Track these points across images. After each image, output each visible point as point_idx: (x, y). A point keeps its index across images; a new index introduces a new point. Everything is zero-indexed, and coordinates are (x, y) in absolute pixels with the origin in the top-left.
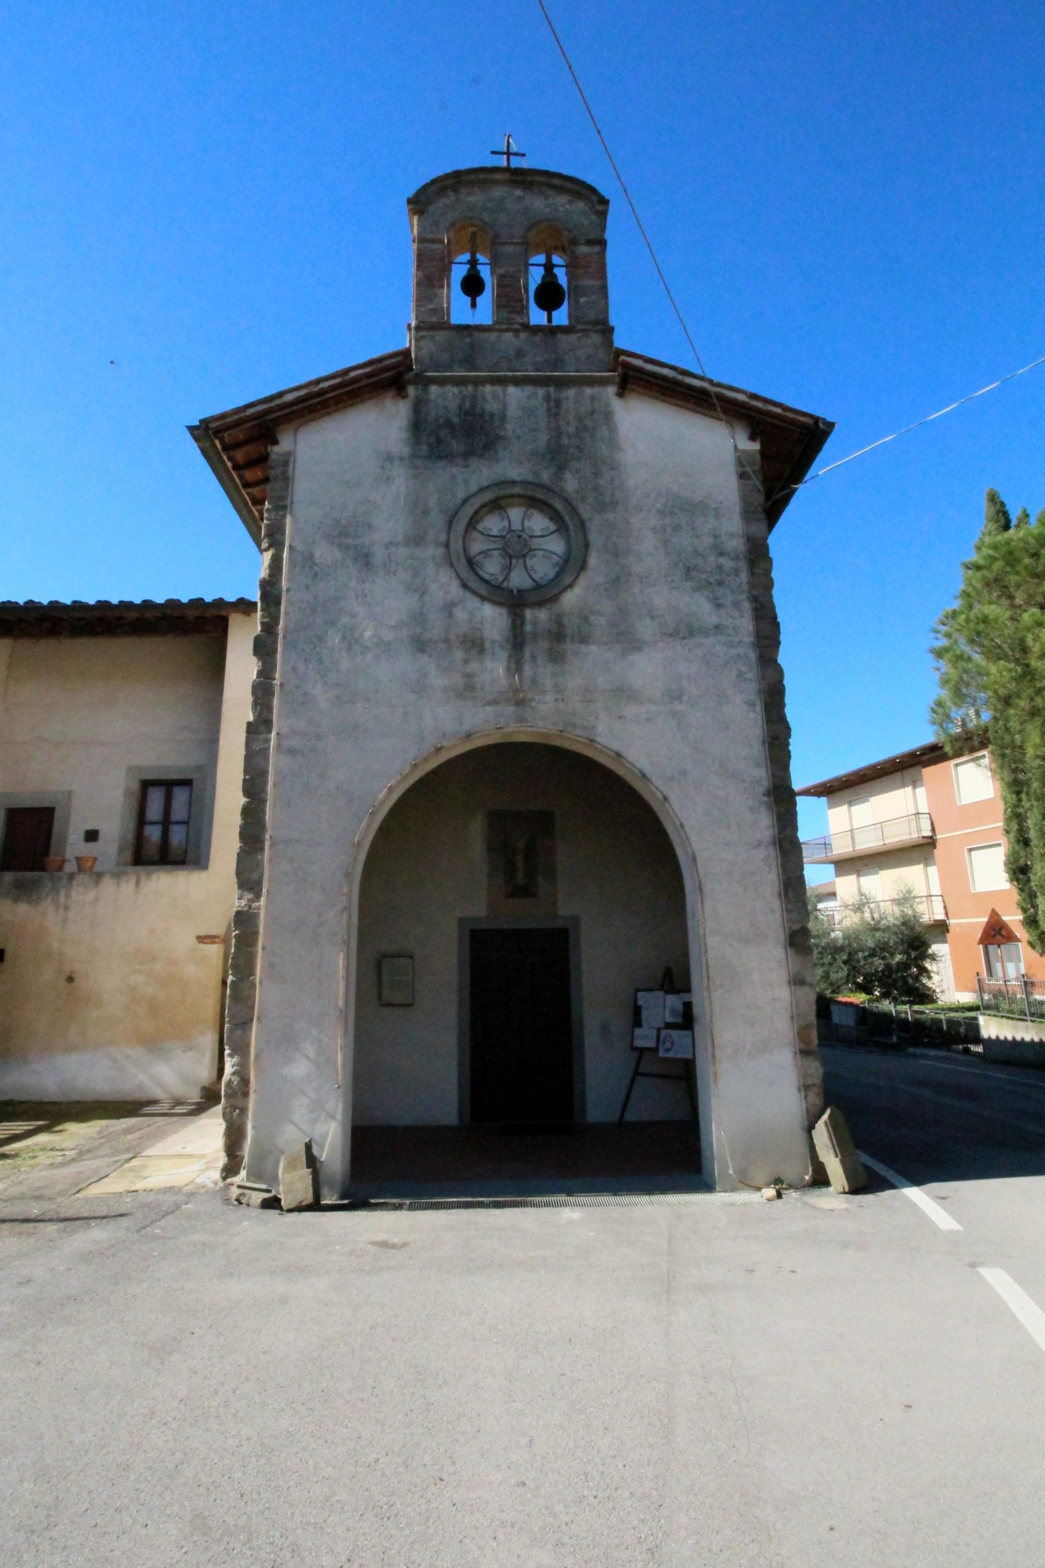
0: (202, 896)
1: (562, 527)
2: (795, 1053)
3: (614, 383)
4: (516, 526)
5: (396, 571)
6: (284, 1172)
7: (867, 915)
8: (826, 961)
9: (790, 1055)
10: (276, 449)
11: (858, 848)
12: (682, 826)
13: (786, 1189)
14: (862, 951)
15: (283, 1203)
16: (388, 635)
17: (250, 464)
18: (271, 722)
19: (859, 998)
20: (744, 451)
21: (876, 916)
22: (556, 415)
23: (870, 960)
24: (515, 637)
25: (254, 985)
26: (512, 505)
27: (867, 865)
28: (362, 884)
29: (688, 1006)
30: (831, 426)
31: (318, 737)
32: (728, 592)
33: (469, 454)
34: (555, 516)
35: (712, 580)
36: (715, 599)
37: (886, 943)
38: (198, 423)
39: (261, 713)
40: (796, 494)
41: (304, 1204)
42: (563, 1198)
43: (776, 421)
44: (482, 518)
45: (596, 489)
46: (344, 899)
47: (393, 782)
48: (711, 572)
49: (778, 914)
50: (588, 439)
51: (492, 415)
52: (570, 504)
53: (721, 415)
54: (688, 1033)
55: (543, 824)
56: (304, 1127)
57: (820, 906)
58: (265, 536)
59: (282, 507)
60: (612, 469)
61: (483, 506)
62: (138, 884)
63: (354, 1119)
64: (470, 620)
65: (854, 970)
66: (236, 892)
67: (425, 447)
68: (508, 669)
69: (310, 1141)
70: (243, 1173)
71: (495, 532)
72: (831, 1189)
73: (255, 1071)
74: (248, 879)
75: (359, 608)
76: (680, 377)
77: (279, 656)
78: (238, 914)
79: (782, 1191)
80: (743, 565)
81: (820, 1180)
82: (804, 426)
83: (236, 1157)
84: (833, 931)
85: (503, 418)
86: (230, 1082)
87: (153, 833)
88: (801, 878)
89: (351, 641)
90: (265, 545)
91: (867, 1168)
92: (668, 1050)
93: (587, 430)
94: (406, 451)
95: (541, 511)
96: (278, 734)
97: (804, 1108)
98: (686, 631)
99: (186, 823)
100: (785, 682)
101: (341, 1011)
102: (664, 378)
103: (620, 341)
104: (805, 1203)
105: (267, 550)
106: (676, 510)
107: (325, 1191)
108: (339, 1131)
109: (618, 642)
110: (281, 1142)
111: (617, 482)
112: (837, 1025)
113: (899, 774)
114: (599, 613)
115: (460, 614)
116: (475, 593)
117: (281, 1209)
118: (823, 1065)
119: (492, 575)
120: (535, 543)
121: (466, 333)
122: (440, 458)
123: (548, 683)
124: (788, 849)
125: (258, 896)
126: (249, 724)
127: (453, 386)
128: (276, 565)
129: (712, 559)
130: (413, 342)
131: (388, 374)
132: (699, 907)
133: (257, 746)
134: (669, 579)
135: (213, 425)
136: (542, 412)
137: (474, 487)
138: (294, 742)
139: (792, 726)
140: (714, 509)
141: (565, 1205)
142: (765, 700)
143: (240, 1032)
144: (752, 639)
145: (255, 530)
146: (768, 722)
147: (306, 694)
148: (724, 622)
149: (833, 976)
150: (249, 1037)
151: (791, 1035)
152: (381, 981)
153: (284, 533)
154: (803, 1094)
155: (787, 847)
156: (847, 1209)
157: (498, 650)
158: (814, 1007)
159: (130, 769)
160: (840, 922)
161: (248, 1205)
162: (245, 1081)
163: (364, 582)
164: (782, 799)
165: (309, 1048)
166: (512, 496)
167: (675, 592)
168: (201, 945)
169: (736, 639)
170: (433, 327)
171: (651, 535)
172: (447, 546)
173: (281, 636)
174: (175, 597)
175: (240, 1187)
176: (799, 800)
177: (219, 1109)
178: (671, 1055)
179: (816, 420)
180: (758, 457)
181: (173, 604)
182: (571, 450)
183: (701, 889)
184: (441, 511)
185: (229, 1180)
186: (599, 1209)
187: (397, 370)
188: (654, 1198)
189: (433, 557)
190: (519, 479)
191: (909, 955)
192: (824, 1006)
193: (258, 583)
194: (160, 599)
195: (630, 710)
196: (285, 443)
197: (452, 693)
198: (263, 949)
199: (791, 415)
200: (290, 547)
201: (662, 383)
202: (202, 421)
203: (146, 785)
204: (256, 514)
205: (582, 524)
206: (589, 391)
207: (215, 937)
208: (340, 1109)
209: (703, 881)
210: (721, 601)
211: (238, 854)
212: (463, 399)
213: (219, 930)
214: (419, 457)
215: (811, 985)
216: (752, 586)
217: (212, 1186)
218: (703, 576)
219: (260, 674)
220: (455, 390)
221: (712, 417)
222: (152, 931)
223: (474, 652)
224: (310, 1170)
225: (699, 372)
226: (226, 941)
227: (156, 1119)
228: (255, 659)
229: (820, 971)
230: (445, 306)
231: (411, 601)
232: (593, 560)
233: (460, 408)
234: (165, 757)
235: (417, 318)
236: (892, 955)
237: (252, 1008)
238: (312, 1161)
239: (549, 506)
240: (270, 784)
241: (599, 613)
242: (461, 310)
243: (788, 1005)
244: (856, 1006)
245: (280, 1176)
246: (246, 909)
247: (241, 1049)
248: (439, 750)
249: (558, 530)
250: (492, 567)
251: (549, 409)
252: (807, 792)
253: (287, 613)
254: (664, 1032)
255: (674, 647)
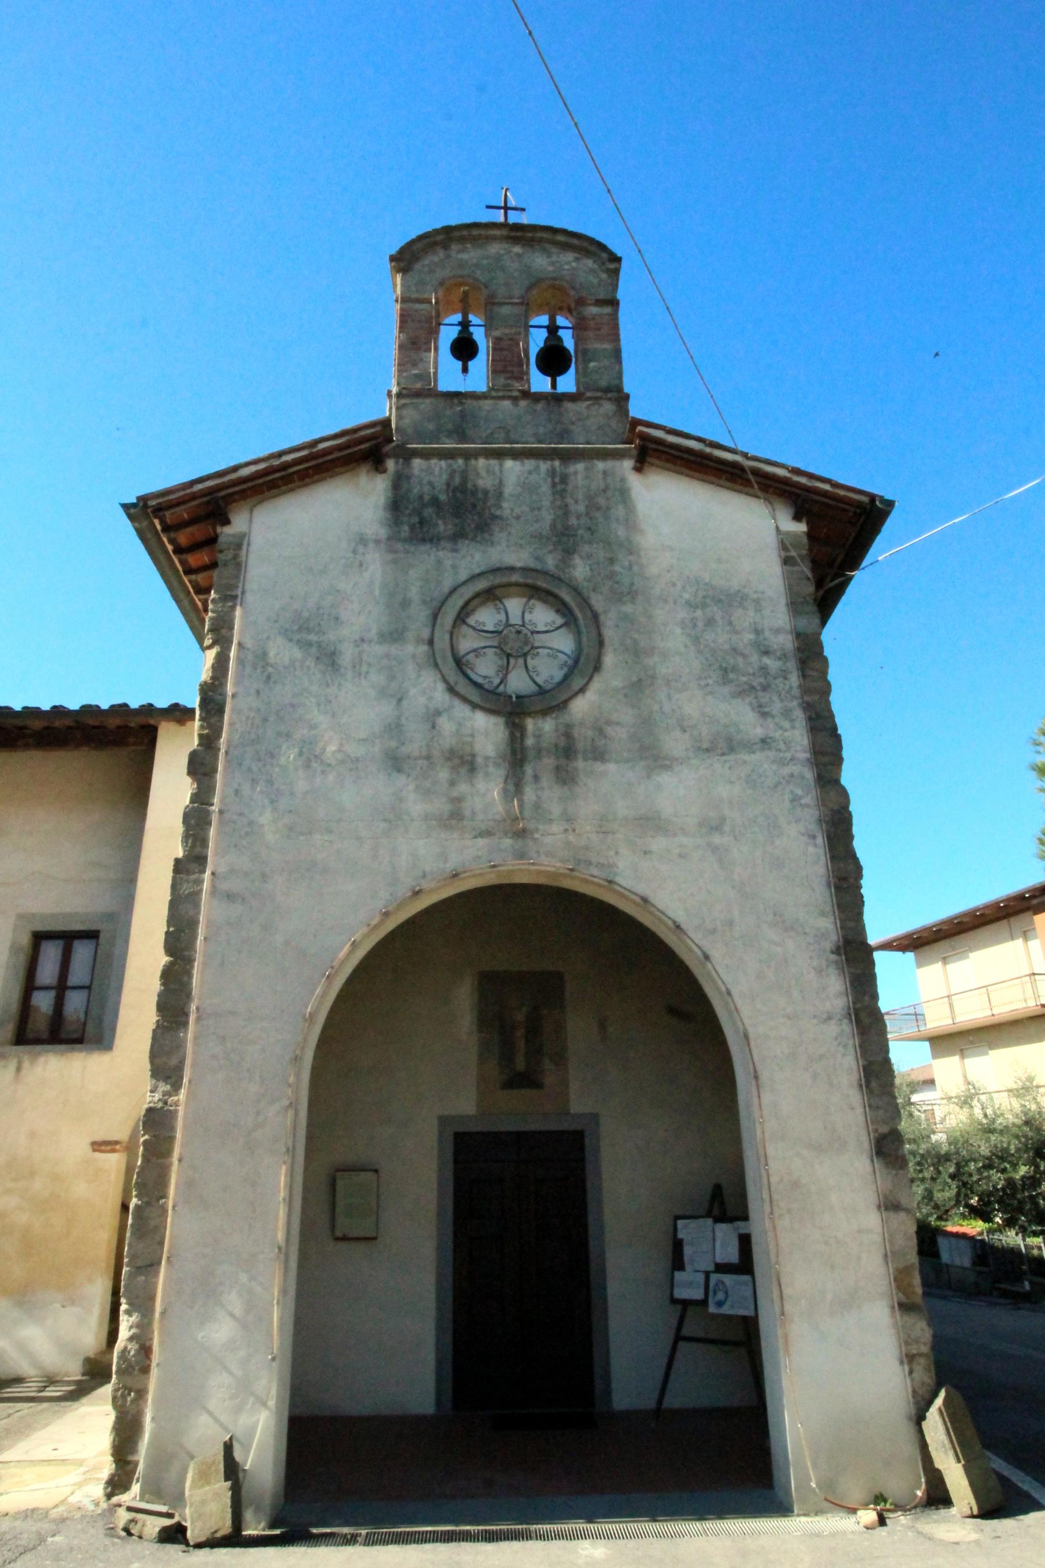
0: (106, 1085)
1: (569, 619)
2: (893, 1307)
3: (630, 457)
4: (515, 619)
5: (368, 672)
6: (193, 1487)
7: (978, 1112)
8: (927, 1174)
9: (886, 1311)
10: (227, 530)
11: (958, 1020)
12: (729, 993)
13: (889, 1510)
14: (975, 1161)
15: (189, 1534)
16: (353, 749)
17: (195, 547)
18: (205, 858)
19: (975, 1227)
20: (788, 533)
21: (989, 1112)
22: (562, 493)
23: (985, 1174)
24: (514, 752)
25: (165, 1211)
26: (508, 596)
27: (972, 1043)
28: (314, 1069)
29: (745, 1242)
30: (890, 504)
31: (264, 877)
32: (775, 698)
33: (458, 536)
34: (562, 608)
35: (755, 684)
36: (760, 706)
37: (1005, 1150)
38: (135, 501)
39: (193, 846)
40: (853, 583)
41: (219, 1535)
42: (581, 1525)
43: (793, 489)
44: (473, 611)
45: (611, 576)
46: (290, 1091)
47: (357, 936)
48: (754, 674)
49: (859, 1110)
50: (601, 520)
51: (486, 492)
52: (580, 594)
53: (760, 493)
54: (747, 1278)
55: (547, 990)
56: (223, 1418)
57: (915, 1098)
58: (209, 631)
59: (231, 597)
60: (631, 554)
61: (477, 595)
62: (19, 1069)
63: (293, 1405)
64: (458, 731)
65: (966, 1187)
66: (148, 1082)
67: (406, 528)
68: (505, 791)
69: (231, 1439)
70: (136, 1488)
71: (490, 627)
72: (954, 1511)
73: (160, 1336)
74: (165, 1065)
75: (317, 716)
76: (708, 450)
77: (219, 776)
78: (150, 1111)
79: (886, 1514)
80: (792, 665)
81: (938, 1497)
82: (859, 505)
83: (129, 1463)
84: (934, 1133)
85: (500, 495)
86: (125, 1350)
87: (43, 1002)
88: (887, 1062)
89: (310, 757)
90: (208, 642)
91: (1003, 1479)
92: (720, 1304)
93: (599, 509)
94: (383, 532)
95: (546, 602)
96: (213, 874)
97: (910, 1390)
98: (726, 744)
99: (89, 988)
100: (851, 809)
101: (280, 1248)
102: (689, 451)
103: (636, 410)
104: (919, 1533)
105: (209, 647)
106: (708, 601)
107: (248, 1515)
108: (272, 1422)
109: (641, 758)
110: (191, 1440)
111: (635, 568)
112: (947, 1265)
113: (1005, 921)
114: (618, 724)
115: (446, 725)
116: (465, 700)
117: (187, 1544)
118: (930, 1323)
119: (485, 677)
120: (538, 640)
121: (456, 401)
122: (423, 540)
123: (556, 810)
124: (867, 1023)
125: (176, 1087)
126: (177, 861)
127: (440, 459)
128: (220, 666)
129: (754, 658)
130: (394, 410)
131: (363, 446)
132: (755, 1100)
133: (186, 889)
134: (703, 683)
135: (152, 503)
136: (545, 488)
137: (463, 576)
138: (234, 885)
139: (863, 862)
140: (754, 600)
141: (583, 1536)
142: (828, 831)
143: (143, 1278)
144: (808, 755)
145: (197, 623)
146: (833, 858)
147: (251, 823)
148: (772, 735)
149: (938, 1196)
150: (156, 1284)
151: (886, 1282)
152: (334, 1207)
153: (232, 628)
154: (907, 1368)
155: (866, 1021)
156: (977, 1542)
157: (491, 769)
158: (914, 1241)
159: (20, 917)
160: (943, 1120)
161: (140, 1537)
162: (146, 1350)
163: (328, 686)
164: (855, 956)
165: (234, 1301)
166: (509, 585)
167: (709, 698)
168: (97, 1154)
169: (788, 755)
170: (418, 394)
171: (678, 631)
172: (431, 642)
173: (222, 751)
174: (93, 702)
175: (130, 1509)
176: (877, 956)
177: (107, 1390)
178: (726, 1310)
179: (873, 498)
180: (805, 540)
181: (89, 710)
182: (580, 532)
183: (756, 1078)
184: (424, 602)
185: (115, 1499)
186: (632, 1543)
187: (374, 442)
188: (709, 1525)
189: (414, 656)
190: (519, 565)
191: (1037, 1166)
192: (928, 1238)
193: (198, 687)
194: (74, 705)
195: (658, 843)
196: (238, 522)
197: (434, 822)
198: (180, 1160)
199: (842, 493)
200: (240, 644)
201: (686, 456)
202: (139, 498)
203: (39, 938)
204: (199, 604)
205: (595, 616)
206: (600, 465)
207: (117, 1143)
208: (274, 1392)
209: (759, 1067)
210: (767, 710)
211: (154, 1031)
212: (452, 474)
213: (122, 1134)
214: (400, 540)
215: (907, 1211)
216: (805, 690)
217: (91, 1507)
218: (744, 679)
219: (195, 798)
220: (443, 463)
221: (747, 494)
222: (32, 1135)
223: (463, 771)
224: (229, 1483)
225: (731, 445)
226: (130, 1148)
227: (20, 1405)
228: (188, 780)
229: (919, 1190)
230: (432, 370)
231: (386, 709)
232: (609, 659)
233: (448, 484)
234: (66, 902)
235: (398, 384)
236: (1015, 1166)
237: (161, 1243)
238: (232, 1470)
239: (556, 596)
240: (200, 938)
241: (618, 724)
242: (449, 375)
243: (878, 1238)
244: (972, 1239)
245: (187, 1493)
246: (160, 1105)
247: (143, 1305)
248: (416, 893)
249: (565, 625)
250: (486, 668)
251: (554, 485)
252: (887, 946)
253: (231, 724)
254: (714, 1278)
255: (711, 765)
